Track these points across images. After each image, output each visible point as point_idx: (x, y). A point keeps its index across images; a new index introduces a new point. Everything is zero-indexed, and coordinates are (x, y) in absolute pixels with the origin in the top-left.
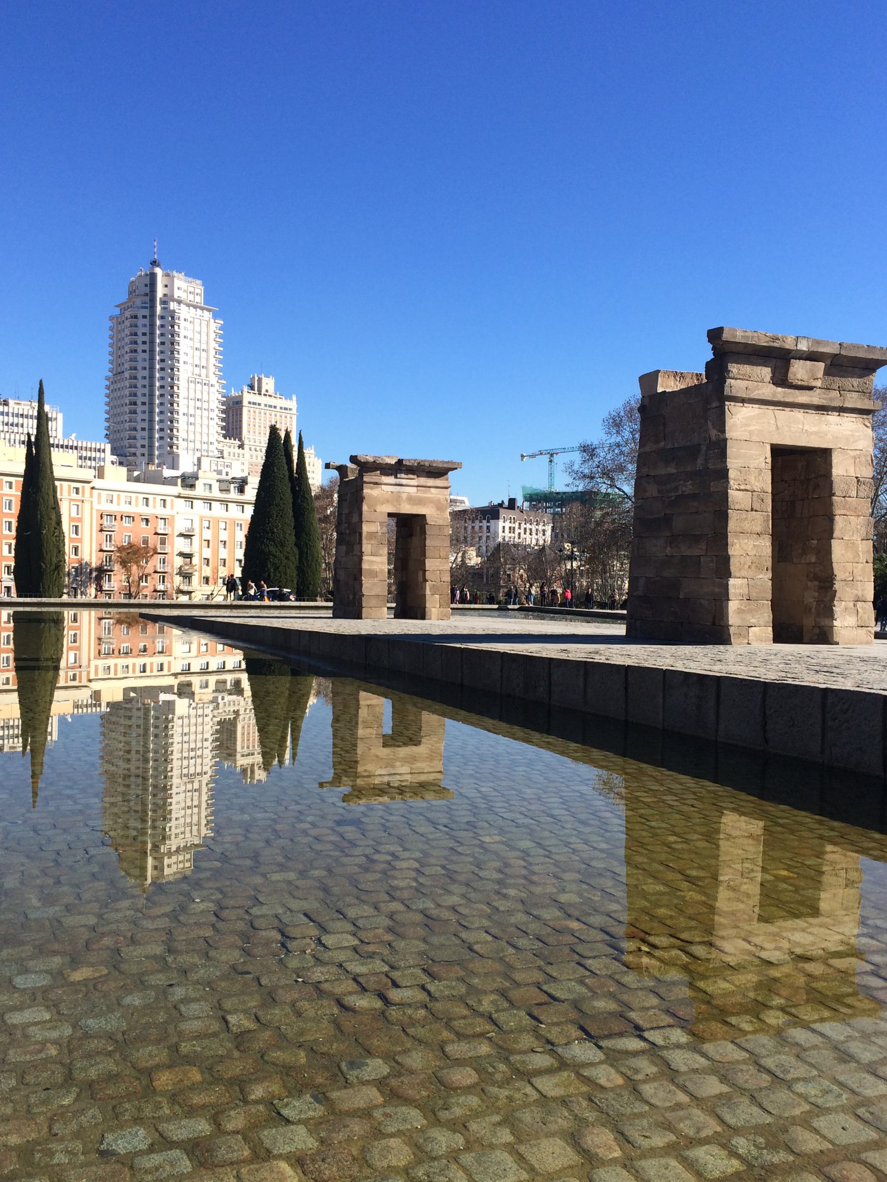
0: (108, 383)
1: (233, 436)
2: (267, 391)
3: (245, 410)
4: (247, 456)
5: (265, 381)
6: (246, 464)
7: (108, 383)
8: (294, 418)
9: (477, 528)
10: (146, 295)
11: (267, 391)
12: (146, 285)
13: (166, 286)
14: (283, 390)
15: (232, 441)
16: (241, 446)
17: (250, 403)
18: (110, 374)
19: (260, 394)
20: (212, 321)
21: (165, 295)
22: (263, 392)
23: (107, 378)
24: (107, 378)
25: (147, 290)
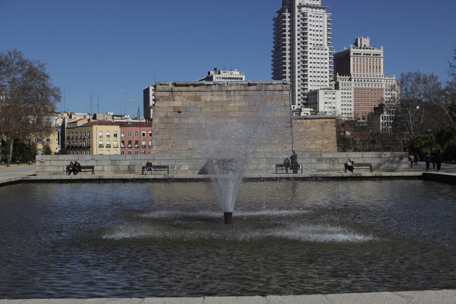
0: (273, 54)
2: (365, 46)
3: (352, 58)
4: (353, 85)
5: (363, 40)
6: (353, 89)
7: (273, 54)
8: (382, 59)
11: (365, 46)
14: (374, 45)
15: (344, 77)
16: (350, 80)
17: (354, 54)
18: (274, 49)
19: (360, 48)
20: (326, 14)
21: (300, 4)
22: (363, 46)
23: (272, 51)
24: (272, 51)
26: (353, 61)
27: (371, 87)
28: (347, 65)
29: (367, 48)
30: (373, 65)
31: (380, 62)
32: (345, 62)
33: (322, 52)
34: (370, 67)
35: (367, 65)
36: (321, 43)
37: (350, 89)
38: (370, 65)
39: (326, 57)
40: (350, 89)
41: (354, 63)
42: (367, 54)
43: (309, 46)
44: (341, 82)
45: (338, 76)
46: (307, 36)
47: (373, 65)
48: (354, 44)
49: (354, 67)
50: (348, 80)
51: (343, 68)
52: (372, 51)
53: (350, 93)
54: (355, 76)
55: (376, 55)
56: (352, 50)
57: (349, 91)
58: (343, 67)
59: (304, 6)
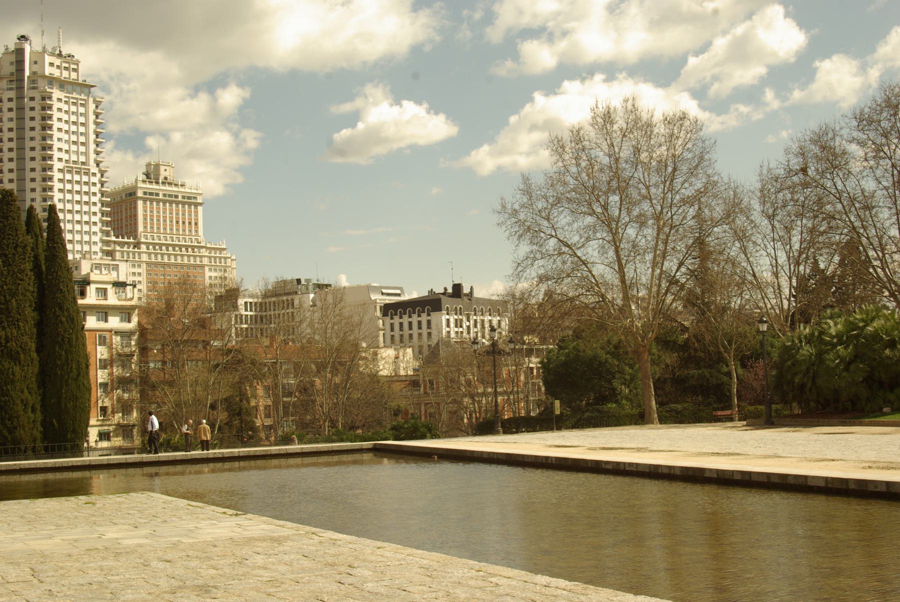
1: (126, 233)
2: (166, 178)
3: (140, 203)
6: (144, 266)
9: (406, 326)
10: (12, 74)
11: (166, 178)
12: (12, 63)
13: (36, 63)
17: (145, 193)
19: (157, 183)
25: (13, 69)
26: (144, 207)
27: (180, 262)
28: (131, 216)
29: (170, 184)
30: (184, 219)
31: (196, 212)
32: (126, 209)
33: (85, 179)
34: (177, 222)
35: (171, 218)
36: (82, 159)
37: (139, 266)
38: (178, 218)
39: (94, 189)
40: (139, 266)
41: (146, 211)
42: (170, 196)
43: (57, 165)
44: (119, 251)
45: (114, 238)
46: (51, 143)
47: (184, 219)
48: (144, 174)
49: (145, 219)
50: (134, 247)
51: (122, 223)
52: (181, 189)
53: (140, 274)
54: (147, 239)
55: (189, 198)
56: (140, 185)
57: (137, 270)
58: (122, 219)
59: (44, 77)
